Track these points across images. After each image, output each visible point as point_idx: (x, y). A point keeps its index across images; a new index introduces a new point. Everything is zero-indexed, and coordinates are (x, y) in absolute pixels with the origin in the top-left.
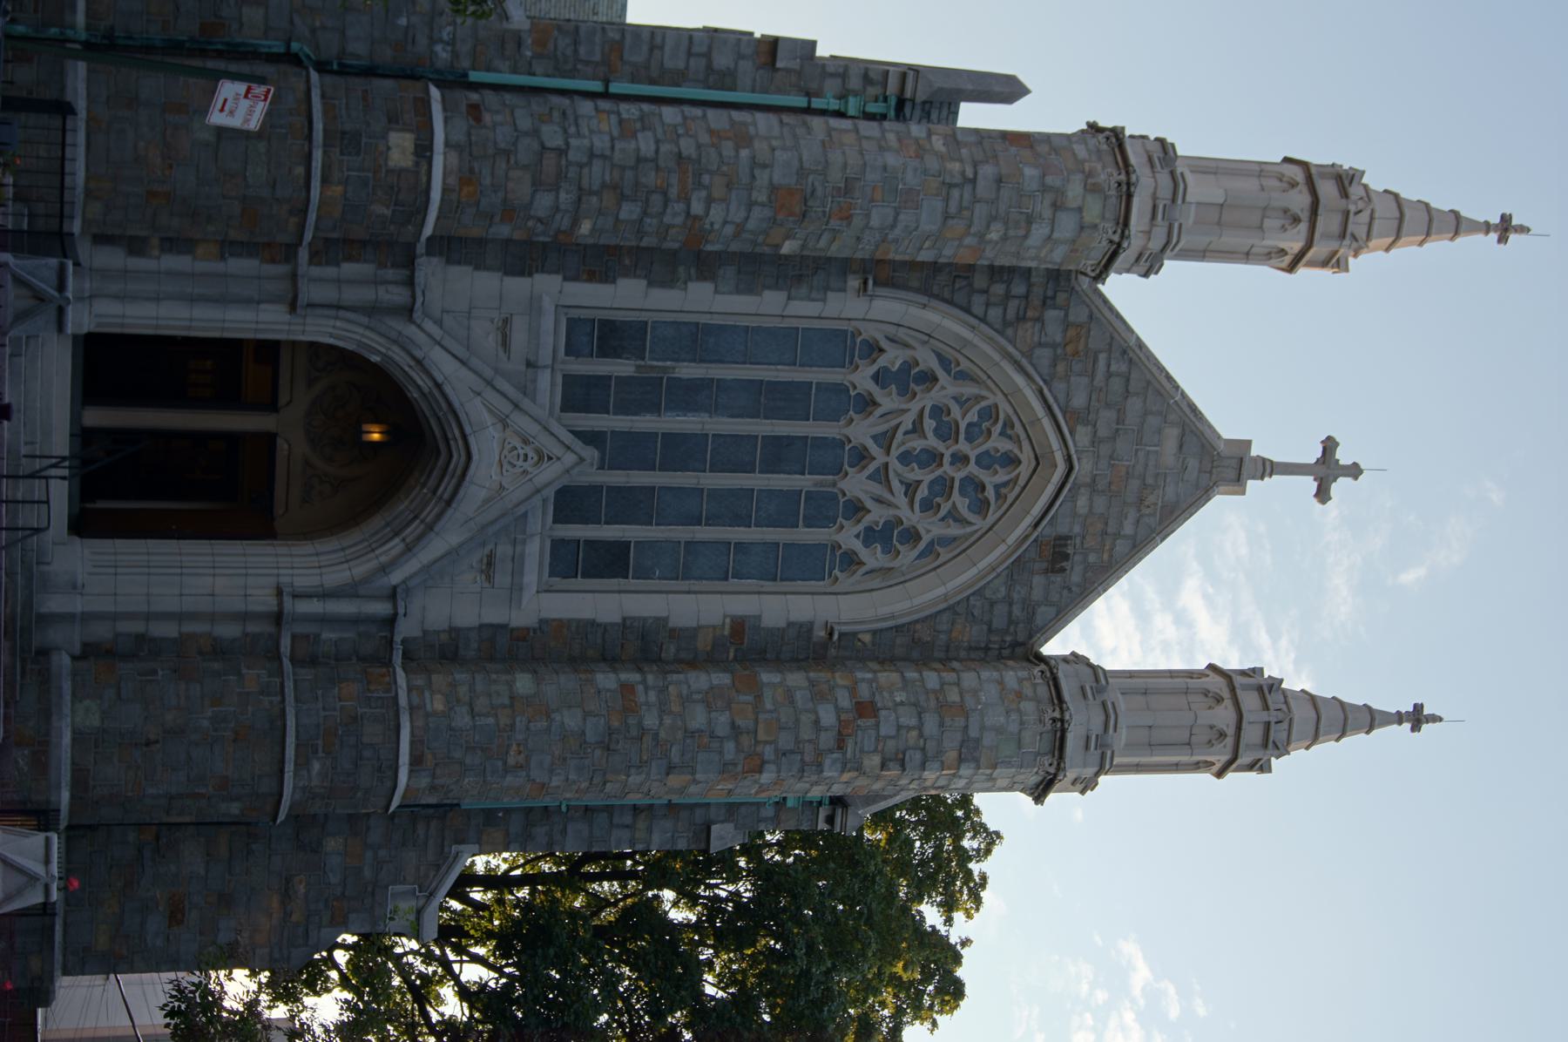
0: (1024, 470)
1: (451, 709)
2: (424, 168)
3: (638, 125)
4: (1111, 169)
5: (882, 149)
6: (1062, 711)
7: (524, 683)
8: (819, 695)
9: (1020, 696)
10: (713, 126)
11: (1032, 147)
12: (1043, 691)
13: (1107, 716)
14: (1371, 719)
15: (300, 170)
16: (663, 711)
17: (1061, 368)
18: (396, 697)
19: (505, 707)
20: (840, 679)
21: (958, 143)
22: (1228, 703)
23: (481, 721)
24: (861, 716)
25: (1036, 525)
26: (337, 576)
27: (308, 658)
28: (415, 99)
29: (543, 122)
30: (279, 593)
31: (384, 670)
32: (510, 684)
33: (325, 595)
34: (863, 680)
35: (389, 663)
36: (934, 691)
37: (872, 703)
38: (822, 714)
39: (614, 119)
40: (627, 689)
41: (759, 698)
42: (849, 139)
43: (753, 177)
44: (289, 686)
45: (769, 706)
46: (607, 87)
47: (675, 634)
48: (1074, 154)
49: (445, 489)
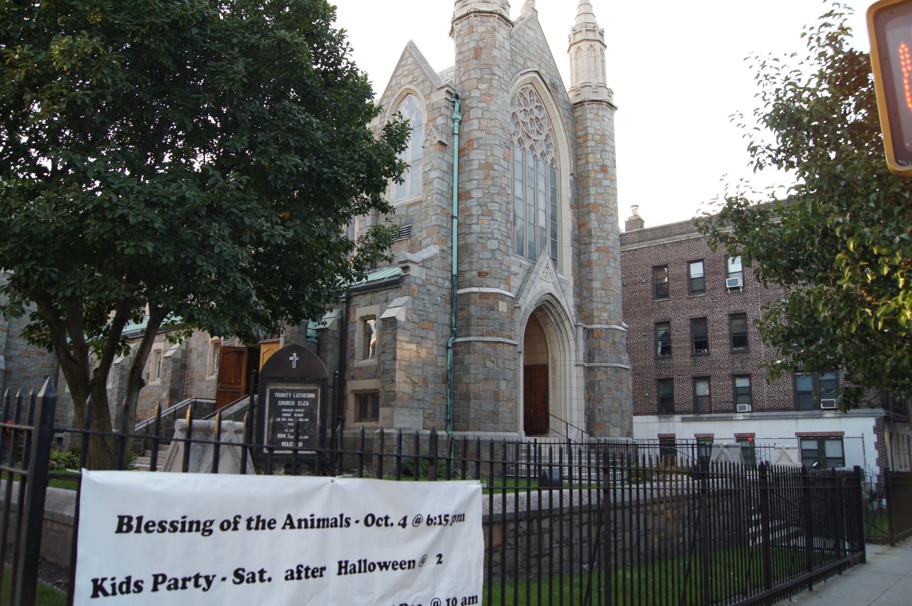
0: (534, 90)
2: (506, 298)
3: (485, 208)
4: (491, 19)
5: (488, 110)
7: (596, 285)
8: (599, 184)
9: (597, 115)
10: (482, 177)
11: (481, 48)
12: (595, 106)
13: (585, 86)
15: (511, 347)
17: (515, 64)
20: (592, 175)
21: (481, 78)
22: (593, 43)
23: (612, 301)
24: (606, 171)
25: (549, 91)
26: (572, 343)
28: (480, 298)
30: (577, 365)
32: (597, 289)
33: (577, 351)
35: (592, 330)
38: (606, 184)
39: (481, 217)
40: (598, 250)
41: (600, 205)
42: (484, 123)
44: (603, 364)
45: (604, 202)
47: (573, 230)
49: (555, 303)
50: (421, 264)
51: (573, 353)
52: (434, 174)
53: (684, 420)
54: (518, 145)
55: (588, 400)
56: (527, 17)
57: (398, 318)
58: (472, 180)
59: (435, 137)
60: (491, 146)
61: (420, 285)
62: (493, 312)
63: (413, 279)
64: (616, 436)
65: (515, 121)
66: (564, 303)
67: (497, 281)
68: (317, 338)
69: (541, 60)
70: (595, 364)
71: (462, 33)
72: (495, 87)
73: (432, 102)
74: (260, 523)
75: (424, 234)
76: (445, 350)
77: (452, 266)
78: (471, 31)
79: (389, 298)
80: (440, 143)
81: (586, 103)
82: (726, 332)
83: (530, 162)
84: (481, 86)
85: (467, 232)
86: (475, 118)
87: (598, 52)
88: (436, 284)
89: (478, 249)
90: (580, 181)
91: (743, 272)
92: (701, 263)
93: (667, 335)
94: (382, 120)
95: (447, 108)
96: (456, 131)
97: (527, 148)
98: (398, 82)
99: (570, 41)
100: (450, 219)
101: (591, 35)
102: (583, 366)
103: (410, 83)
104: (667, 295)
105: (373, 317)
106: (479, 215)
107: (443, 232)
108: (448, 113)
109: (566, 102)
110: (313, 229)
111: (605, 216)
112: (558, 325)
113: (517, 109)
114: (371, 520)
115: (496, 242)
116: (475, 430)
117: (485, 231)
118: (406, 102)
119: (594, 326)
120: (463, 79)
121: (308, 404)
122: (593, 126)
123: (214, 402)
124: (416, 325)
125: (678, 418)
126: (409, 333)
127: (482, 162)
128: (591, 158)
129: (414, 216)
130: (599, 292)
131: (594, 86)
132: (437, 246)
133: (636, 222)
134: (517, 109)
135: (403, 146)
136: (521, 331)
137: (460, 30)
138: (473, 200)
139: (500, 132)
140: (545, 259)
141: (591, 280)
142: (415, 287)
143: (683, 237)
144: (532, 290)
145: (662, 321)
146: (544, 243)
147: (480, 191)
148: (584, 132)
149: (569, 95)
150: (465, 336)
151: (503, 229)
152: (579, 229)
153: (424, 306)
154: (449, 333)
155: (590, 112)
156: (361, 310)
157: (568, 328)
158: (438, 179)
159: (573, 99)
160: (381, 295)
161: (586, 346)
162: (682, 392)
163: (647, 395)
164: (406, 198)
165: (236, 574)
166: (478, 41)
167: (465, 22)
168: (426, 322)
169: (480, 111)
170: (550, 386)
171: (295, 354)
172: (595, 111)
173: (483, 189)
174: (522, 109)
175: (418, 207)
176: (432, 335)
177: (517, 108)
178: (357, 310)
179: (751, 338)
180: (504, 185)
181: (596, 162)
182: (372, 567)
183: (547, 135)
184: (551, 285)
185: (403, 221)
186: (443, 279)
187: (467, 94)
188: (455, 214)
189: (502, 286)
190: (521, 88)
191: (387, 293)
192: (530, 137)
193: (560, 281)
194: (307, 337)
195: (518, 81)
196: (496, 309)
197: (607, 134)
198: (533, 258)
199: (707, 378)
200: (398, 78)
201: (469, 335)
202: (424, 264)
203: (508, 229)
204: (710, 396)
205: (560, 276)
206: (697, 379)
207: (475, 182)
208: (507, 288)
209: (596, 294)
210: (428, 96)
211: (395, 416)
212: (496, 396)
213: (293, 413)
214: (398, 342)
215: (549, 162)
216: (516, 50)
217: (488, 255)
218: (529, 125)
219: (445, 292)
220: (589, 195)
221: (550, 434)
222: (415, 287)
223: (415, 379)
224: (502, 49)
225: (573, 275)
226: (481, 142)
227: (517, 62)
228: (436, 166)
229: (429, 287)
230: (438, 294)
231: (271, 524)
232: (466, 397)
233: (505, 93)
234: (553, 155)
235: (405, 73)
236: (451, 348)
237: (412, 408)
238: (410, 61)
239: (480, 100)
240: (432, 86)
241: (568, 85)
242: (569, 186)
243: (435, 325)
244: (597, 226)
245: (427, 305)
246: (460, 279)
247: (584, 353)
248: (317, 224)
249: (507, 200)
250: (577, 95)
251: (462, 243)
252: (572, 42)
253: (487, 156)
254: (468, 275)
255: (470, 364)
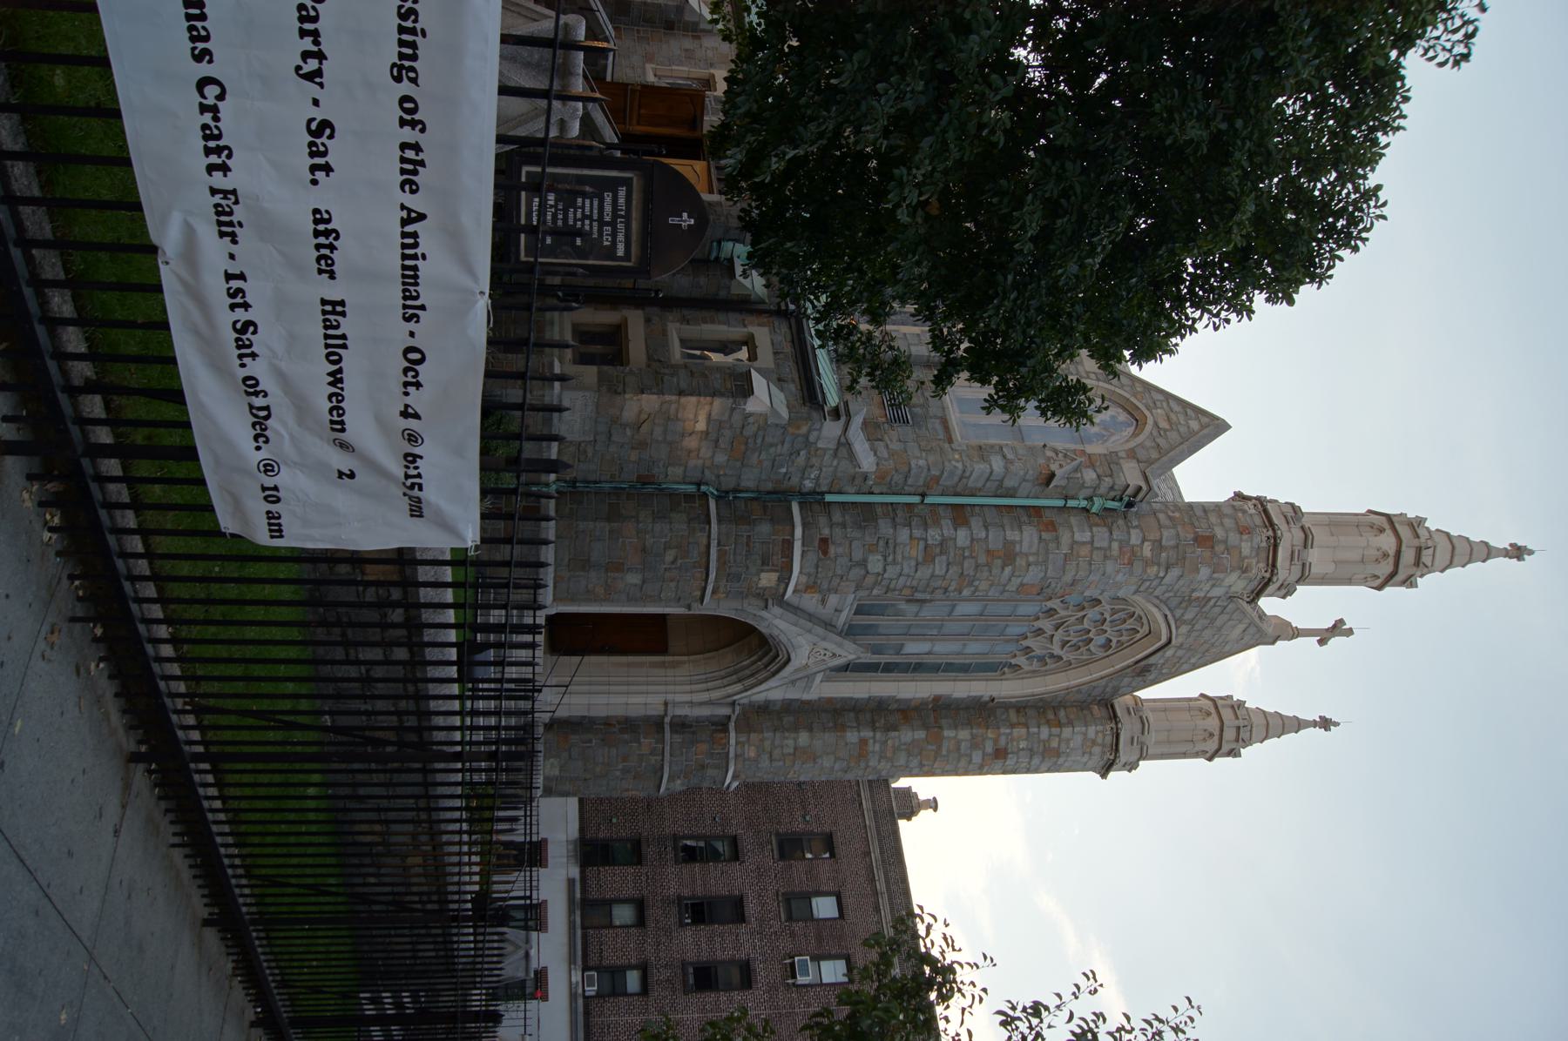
0: (1139, 636)
1: (759, 756)
3: (938, 550)
4: (1262, 565)
5: (1106, 557)
6: (1115, 757)
7: (803, 738)
8: (975, 745)
9: (1094, 742)
10: (991, 547)
11: (1213, 547)
12: (1109, 739)
14: (1298, 725)
15: (698, 593)
16: (881, 757)
17: (1184, 605)
18: (728, 753)
19: (790, 754)
20: (990, 734)
22: (1216, 738)
27: (681, 725)
29: (870, 551)
30: (666, 704)
31: (723, 735)
32: (795, 740)
33: (691, 704)
34: (1004, 734)
35: (725, 730)
36: (1044, 741)
37: (1006, 749)
39: (922, 544)
40: (863, 742)
41: (939, 748)
42: (1085, 551)
43: (1010, 580)
44: (667, 748)
45: (944, 753)
46: (923, 501)
47: (898, 701)
48: (1240, 552)
49: (773, 668)
50: (843, 440)
51: (687, 698)
52: (997, 464)
53: (571, 882)
54: (1045, 609)
55: (607, 722)
56: (1264, 626)
57: (751, 400)
58: (986, 528)
59: (1061, 466)
60: (1046, 561)
61: (807, 438)
62: (759, 562)
63: (817, 426)
64: (546, 768)
65: (1086, 604)
66: (772, 683)
67: (813, 570)
68: (717, 258)
69: (1189, 649)
70: (667, 735)
71: (1240, 515)
72: (1145, 571)
73: (1121, 461)
74: (411, 168)
75: (895, 446)
76: (694, 480)
77: (840, 493)
78: (1244, 531)
79: (785, 385)
80: (1052, 476)
81: (1114, 726)
82: (720, 956)
83: (1015, 630)
84: (1147, 547)
85: (897, 520)
86: (1093, 537)
87: (1200, 747)
88: (808, 466)
89: (867, 538)
90: (981, 712)
91: (822, 985)
92: (836, 914)
93: (715, 856)
94: (1093, 376)
95: (1112, 488)
96: (1071, 503)
97: (1038, 624)
98: (1158, 404)
99: (1221, 698)
100: (920, 490)
101: (1229, 734)
102: (666, 714)
103: (1156, 424)
104: (782, 856)
105: (753, 357)
106: (926, 540)
107: (898, 478)
108: (1102, 490)
109: (1116, 692)
110: (910, 256)
111: (920, 754)
112: (735, 672)
113: (1106, 607)
114: (414, 358)
115: (880, 570)
116: (556, 531)
117: (899, 551)
118: (1123, 417)
119: (733, 735)
120: (1161, 516)
121: (606, 243)
122: (1074, 735)
123: (609, 79)
124: (738, 431)
125: (575, 872)
126: (726, 417)
127: (1018, 546)
128: (1019, 732)
129: (927, 429)
130: (791, 742)
131: (1143, 739)
132: (874, 468)
133: (910, 805)
134: (1106, 607)
135: (1049, 413)
136: (727, 609)
137: (1244, 512)
138: (952, 531)
139: (1068, 578)
140: (849, 652)
141: (810, 730)
142: (804, 430)
143: (881, 886)
144: (793, 628)
145: (740, 847)
146: (877, 650)
147: (968, 543)
148: (1064, 720)
149: (1127, 697)
150: (718, 514)
151: (902, 580)
152: (898, 710)
153: (771, 445)
154: (724, 488)
155: (1097, 731)
156: (762, 335)
157: (730, 690)
158: (988, 471)
159: (1121, 703)
160: (790, 370)
161: (698, 720)
162: (617, 880)
163: (614, 820)
164: (958, 415)
165: (326, 124)
166: (1225, 542)
167: (1258, 521)
168: (743, 447)
169: (1105, 544)
170: (631, 659)
171: (692, 222)
172: (1099, 740)
173: (971, 547)
174: (1107, 615)
175: (941, 437)
176: (721, 458)
177: (1108, 607)
178: (766, 330)
179: (710, 997)
180: (976, 583)
181: (1012, 740)
182: (334, 357)
183: (1060, 658)
184: (804, 662)
185: (918, 410)
186: (818, 478)
187: (1135, 523)
188: (928, 500)
189: (804, 579)
190: (1142, 614)
191: (793, 381)
192: (1057, 629)
193: (810, 678)
194: (719, 243)
195: (1154, 610)
196: (766, 568)
197: (1061, 760)
198: (850, 632)
199: (641, 921)
200: (1165, 404)
201: (719, 521)
202: (844, 444)
203: (901, 590)
204: (611, 926)
205: (819, 677)
206: (640, 906)
207: (983, 535)
208: (799, 587)
209: (787, 738)
210: (1132, 454)
211: (581, 393)
212: (618, 567)
213: (590, 217)
214: (708, 398)
215: (1013, 661)
216: (1208, 607)
217: (858, 555)
218: (1079, 627)
219: (795, 481)
220: (956, 728)
221: (548, 656)
222: (804, 430)
223: (645, 428)
224: (1211, 583)
225: (820, 699)
226: (1052, 546)
227: (1186, 608)
228: (1012, 468)
229: (802, 453)
230: (790, 470)
231: (410, 185)
232: (613, 515)
233: (1134, 588)
234: (1026, 668)
235: (1173, 416)
236: (699, 489)
237: (596, 422)
238: (1194, 425)
239: (1123, 544)
240: (1150, 462)
241: (1144, 694)
242: (973, 694)
243: (738, 464)
244: (903, 741)
245: (772, 450)
246: (816, 507)
247: (686, 716)
248: (918, 264)
249: (951, 588)
250: (1128, 709)
251: (879, 510)
252: (1220, 703)
253: (1027, 555)
254: (823, 520)
255: (671, 523)
